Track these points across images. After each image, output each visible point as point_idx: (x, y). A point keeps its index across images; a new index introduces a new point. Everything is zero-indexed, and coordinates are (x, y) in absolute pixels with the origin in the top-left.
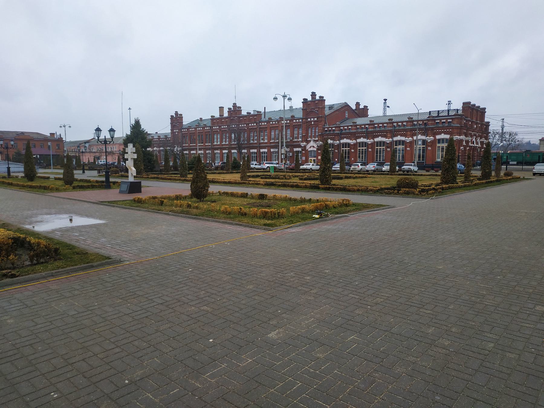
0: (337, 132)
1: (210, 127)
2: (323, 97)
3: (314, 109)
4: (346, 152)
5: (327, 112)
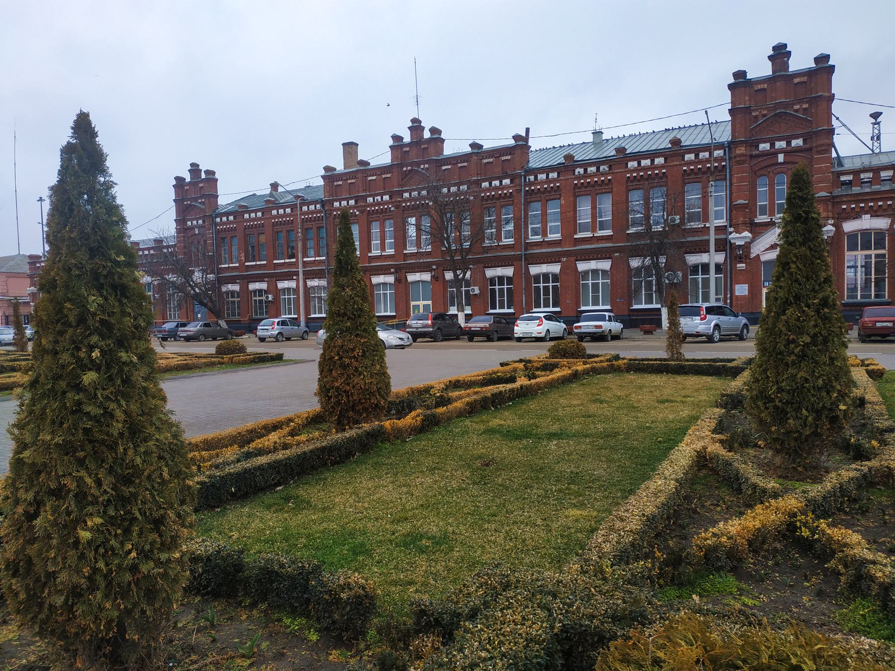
1: (323, 203)
2: (827, 57)
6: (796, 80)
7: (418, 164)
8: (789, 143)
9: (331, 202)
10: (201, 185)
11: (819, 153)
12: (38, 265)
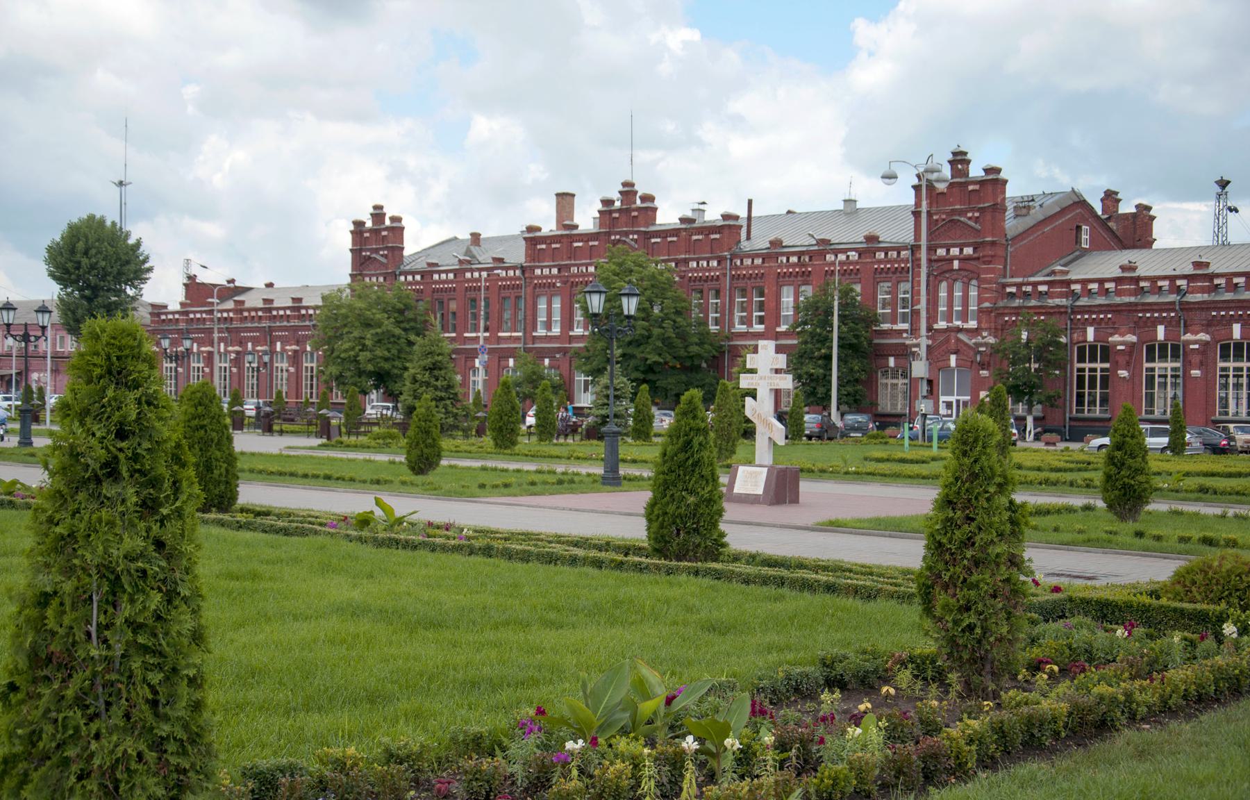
0: (1058, 301)
2: (998, 171)
3: (962, 213)
4: (1093, 380)
5: (1012, 224)
6: (971, 188)
7: (626, 234)
8: (961, 250)
9: (532, 269)
10: (384, 233)
11: (984, 263)
12: (163, 317)
